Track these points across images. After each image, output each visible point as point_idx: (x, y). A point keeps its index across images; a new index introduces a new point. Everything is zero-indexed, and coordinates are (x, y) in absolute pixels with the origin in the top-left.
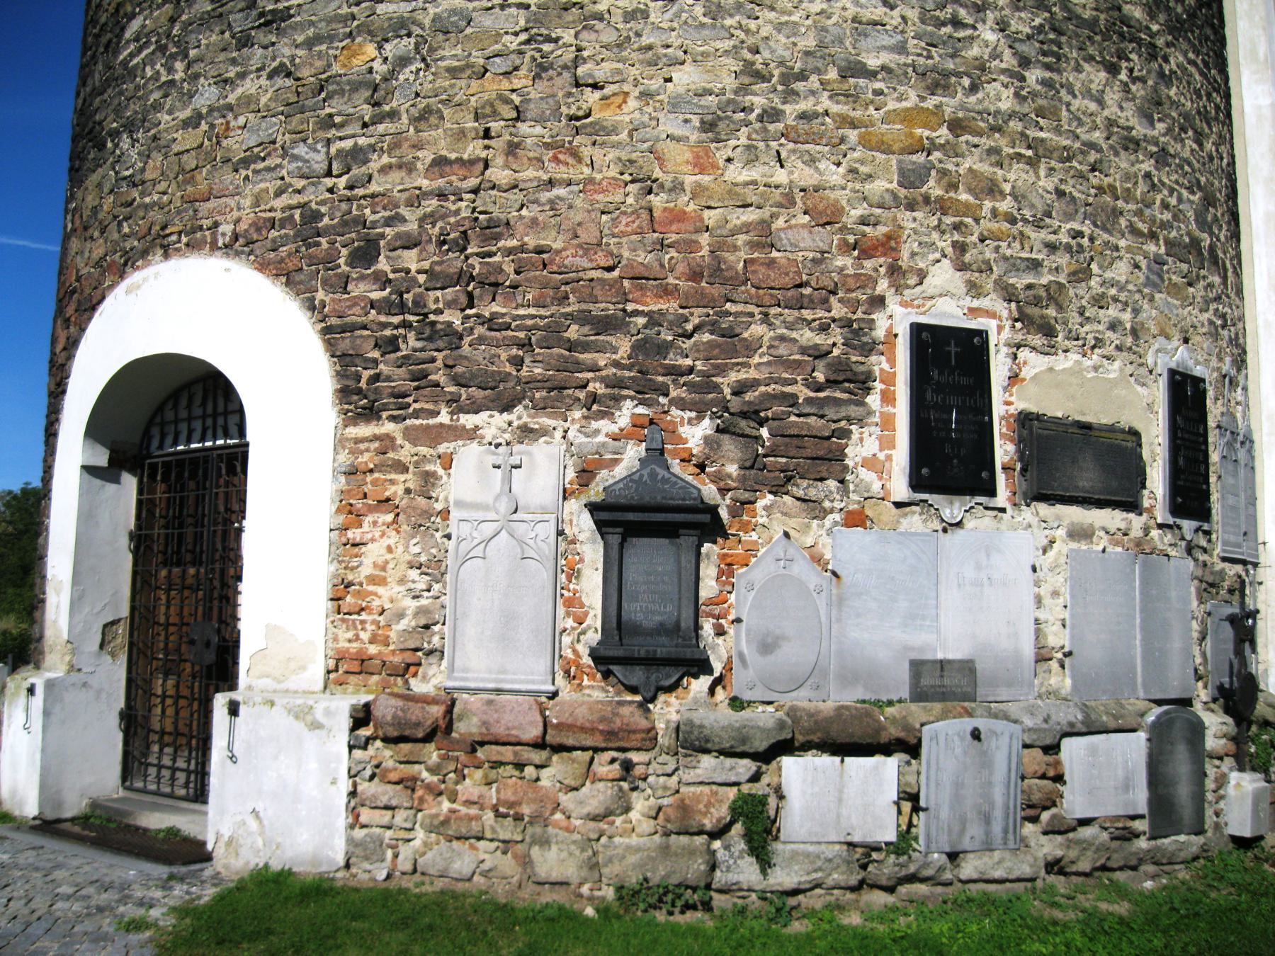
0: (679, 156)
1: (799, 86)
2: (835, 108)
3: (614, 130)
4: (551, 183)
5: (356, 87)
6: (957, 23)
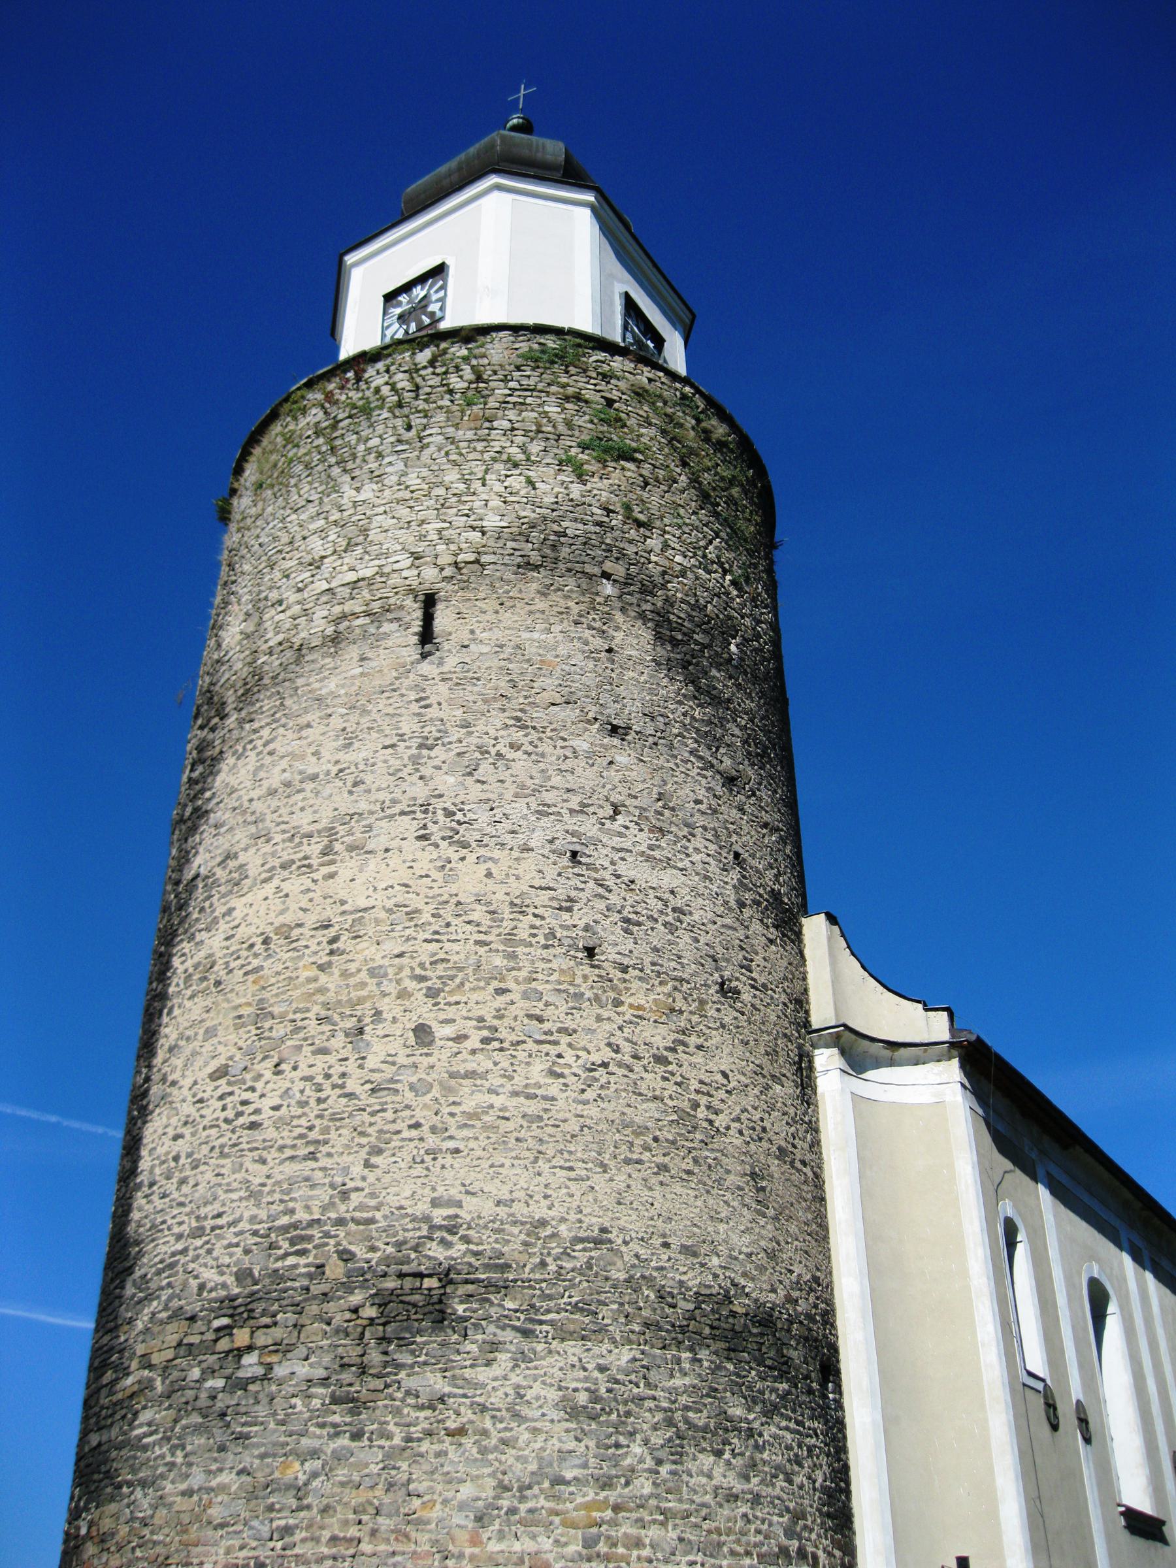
0: (463, 1536)
1: (528, 1493)
2: (548, 1505)
3: (428, 1522)
4: (394, 1553)
5: (288, 1487)
6: (617, 1446)
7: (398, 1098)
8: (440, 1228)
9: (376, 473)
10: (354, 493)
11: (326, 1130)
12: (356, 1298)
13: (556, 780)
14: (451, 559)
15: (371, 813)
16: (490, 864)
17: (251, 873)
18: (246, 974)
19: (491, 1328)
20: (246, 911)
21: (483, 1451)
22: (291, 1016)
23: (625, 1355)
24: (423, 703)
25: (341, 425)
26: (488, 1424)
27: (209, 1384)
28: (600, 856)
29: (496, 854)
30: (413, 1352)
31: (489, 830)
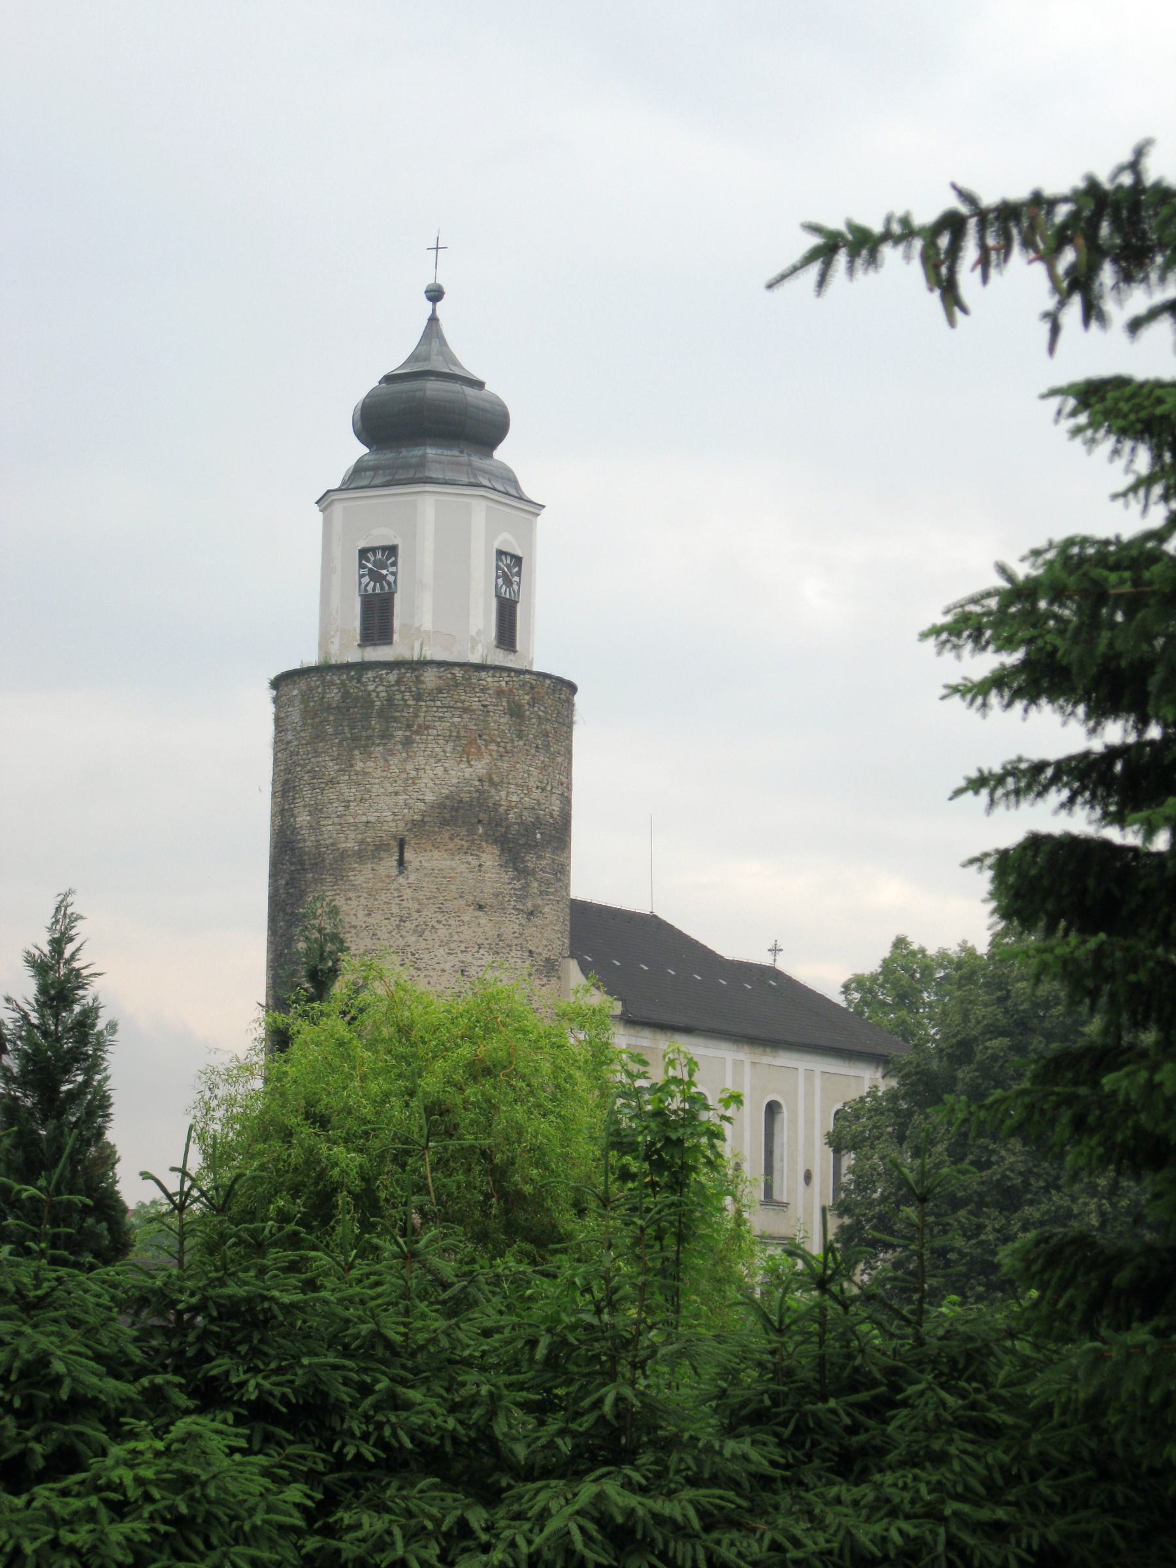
14: (408, 818)
28: (472, 971)
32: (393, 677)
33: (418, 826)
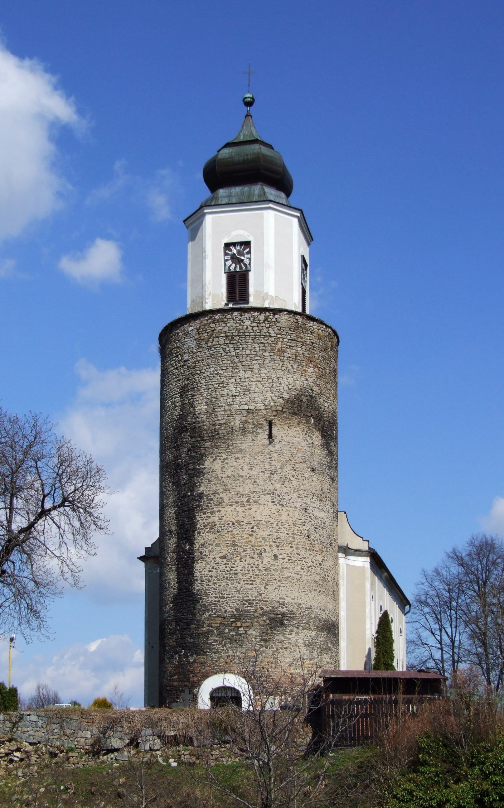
6: (313, 652)
7: (271, 572)
8: (281, 604)
9: (250, 367)
10: (243, 372)
11: (255, 578)
12: (265, 618)
13: (302, 487)
14: (274, 408)
15: (260, 492)
16: (288, 512)
17: (225, 501)
18: (228, 532)
19: (291, 627)
20: (225, 513)
21: (291, 652)
22: (243, 547)
23: (313, 634)
24: (271, 459)
25: (235, 337)
26: (291, 647)
27: (231, 633)
28: (310, 509)
29: (290, 509)
30: (277, 631)
31: (288, 501)
32: (262, 317)
33: (279, 413)
